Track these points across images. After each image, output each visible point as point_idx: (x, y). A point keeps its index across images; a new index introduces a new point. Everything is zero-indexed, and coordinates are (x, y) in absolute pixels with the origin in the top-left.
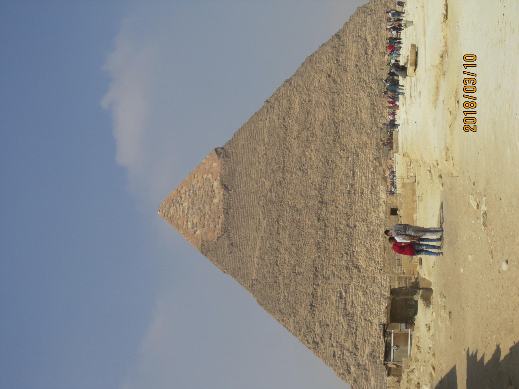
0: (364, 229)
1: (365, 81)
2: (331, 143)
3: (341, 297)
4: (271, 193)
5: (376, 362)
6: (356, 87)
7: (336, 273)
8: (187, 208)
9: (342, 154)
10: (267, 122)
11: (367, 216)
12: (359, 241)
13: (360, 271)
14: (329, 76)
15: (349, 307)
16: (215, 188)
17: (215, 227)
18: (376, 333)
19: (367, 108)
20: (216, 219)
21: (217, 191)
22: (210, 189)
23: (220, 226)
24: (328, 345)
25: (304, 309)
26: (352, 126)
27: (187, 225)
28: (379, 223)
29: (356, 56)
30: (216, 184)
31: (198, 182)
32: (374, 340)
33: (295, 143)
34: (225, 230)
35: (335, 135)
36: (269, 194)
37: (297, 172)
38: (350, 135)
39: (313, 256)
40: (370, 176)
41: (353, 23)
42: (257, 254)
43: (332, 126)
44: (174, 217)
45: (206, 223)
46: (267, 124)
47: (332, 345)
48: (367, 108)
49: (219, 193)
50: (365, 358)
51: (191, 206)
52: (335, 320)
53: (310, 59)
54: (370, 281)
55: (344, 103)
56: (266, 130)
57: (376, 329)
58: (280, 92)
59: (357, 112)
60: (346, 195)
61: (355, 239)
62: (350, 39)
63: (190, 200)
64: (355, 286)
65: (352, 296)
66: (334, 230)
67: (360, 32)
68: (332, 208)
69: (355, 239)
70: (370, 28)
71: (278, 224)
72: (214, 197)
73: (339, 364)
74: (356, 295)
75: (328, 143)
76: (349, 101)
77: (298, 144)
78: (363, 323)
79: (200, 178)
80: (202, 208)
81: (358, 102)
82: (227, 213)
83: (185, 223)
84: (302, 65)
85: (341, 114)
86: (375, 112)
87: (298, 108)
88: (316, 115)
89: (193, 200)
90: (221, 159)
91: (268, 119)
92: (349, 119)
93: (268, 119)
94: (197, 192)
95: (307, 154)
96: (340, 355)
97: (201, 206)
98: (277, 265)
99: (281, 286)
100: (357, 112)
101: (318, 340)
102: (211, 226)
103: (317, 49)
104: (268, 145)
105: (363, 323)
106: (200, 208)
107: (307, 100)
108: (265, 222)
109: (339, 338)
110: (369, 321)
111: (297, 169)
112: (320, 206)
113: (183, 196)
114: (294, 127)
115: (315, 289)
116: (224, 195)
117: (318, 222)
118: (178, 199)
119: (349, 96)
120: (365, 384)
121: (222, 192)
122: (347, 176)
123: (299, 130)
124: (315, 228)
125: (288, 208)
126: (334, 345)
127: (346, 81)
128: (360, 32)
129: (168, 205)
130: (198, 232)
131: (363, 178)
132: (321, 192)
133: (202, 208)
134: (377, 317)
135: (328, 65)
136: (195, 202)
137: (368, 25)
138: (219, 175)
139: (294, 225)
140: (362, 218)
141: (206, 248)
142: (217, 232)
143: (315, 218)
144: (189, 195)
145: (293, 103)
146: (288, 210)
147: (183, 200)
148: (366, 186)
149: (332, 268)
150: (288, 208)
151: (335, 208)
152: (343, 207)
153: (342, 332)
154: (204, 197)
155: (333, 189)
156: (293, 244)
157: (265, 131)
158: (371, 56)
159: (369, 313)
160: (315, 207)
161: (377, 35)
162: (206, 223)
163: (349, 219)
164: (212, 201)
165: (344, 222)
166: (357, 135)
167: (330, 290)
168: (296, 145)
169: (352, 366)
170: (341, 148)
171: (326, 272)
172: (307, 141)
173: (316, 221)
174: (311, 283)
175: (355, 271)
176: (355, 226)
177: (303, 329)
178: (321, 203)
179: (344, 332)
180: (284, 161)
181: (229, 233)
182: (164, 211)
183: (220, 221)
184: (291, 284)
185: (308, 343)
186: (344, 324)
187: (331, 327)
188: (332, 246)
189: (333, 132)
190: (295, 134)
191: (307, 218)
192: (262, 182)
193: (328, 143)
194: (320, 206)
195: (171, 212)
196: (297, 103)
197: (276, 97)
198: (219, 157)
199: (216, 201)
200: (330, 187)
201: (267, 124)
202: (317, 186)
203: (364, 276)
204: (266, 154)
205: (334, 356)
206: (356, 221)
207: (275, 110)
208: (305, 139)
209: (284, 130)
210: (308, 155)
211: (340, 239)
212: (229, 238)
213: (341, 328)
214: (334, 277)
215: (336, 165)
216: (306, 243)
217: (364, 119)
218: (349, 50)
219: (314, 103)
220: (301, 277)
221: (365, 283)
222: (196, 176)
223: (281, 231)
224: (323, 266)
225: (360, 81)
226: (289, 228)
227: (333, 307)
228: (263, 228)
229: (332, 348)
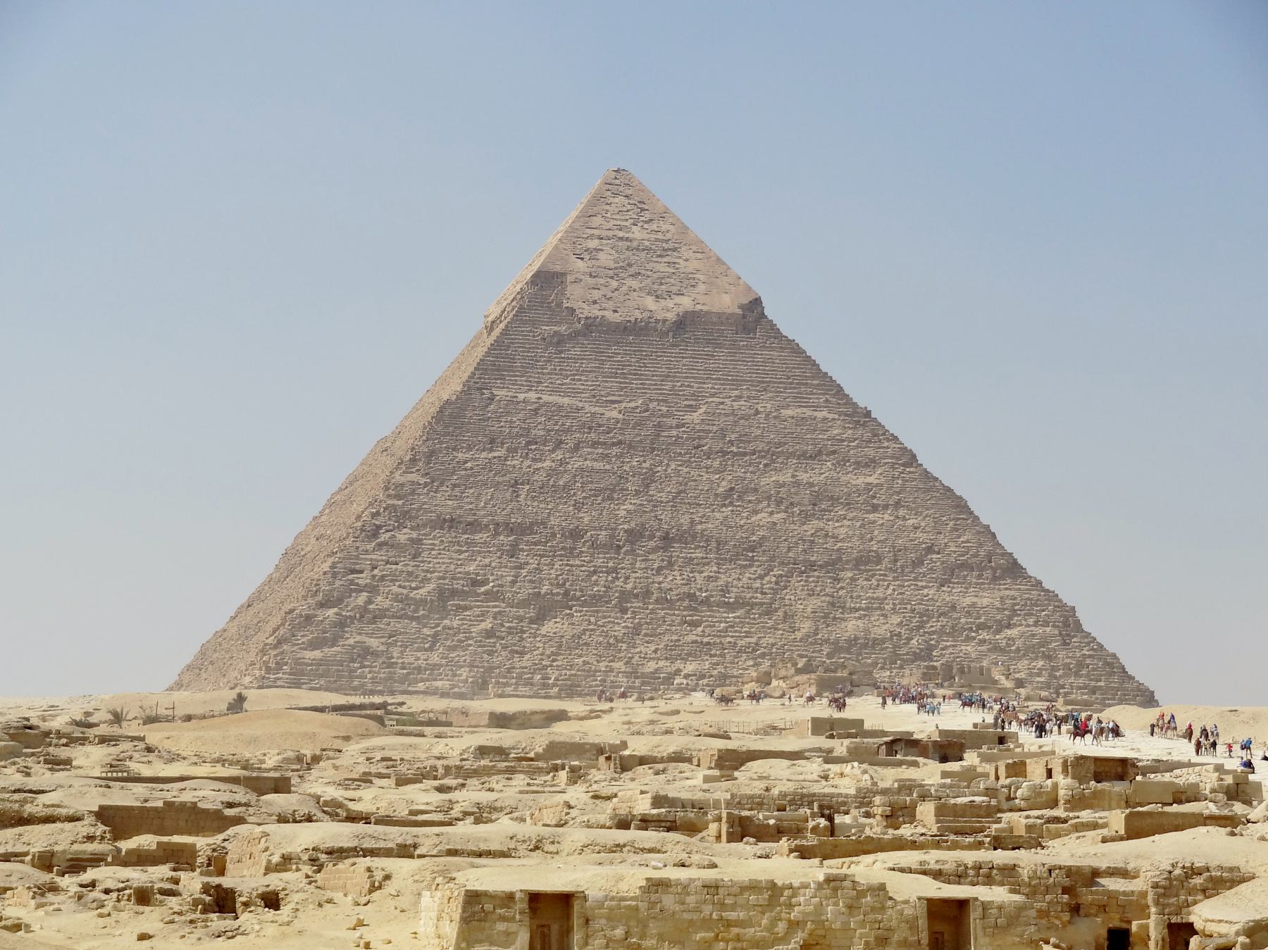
0: (619, 631)
2: (791, 554)
3: (475, 583)
4: (678, 427)
5: (353, 661)
7: (524, 572)
8: (630, 235)
9: (767, 579)
10: (824, 414)
11: (646, 635)
12: (592, 619)
13: (531, 622)
14: (930, 550)
16: (678, 299)
17: (595, 302)
18: (412, 660)
19: (867, 631)
20: (610, 305)
21: (670, 303)
22: (674, 289)
24: (374, 557)
25: (443, 503)
26: (828, 599)
27: (591, 237)
28: (634, 661)
29: (973, 605)
30: (686, 303)
31: (687, 260)
32: (395, 655)
33: (786, 477)
34: (592, 327)
36: (674, 422)
37: (724, 483)
39: (553, 521)
40: (729, 639)
41: (1042, 598)
42: (546, 398)
44: (607, 207)
45: (602, 281)
46: (820, 415)
47: (374, 568)
48: (867, 631)
49: (667, 310)
50: (358, 638)
51: (635, 244)
52: (428, 571)
53: (961, 506)
54: (515, 645)
55: (874, 582)
56: (808, 412)
57: (418, 659)
58: (888, 440)
59: (857, 610)
60: (686, 589)
61: (597, 612)
62: (1007, 592)
63: (647, 243)
64: (500, 612)
65: (478, 607)
66: (611, 564)
68: (656, 560)
69: (597, 612)
71: (614, 444)
72: (657, 297)
73: (338, 583)
74: (483, 615)
75: (789, 549)
76: (879, 593)
77: (783, 485)
78: (426, 631)
80: (632, 270)
81: (878, 612)
82: (625, 328)
83: (596, 232)
84: (949, 490)
85: (850, 574)
86: (861, 648)
87: (858, 482)
88: (846, 523)
89: (647, 249)
90: (739, 311)
91: (831, 416)
92: (841, 593)
93: (831, 416)
94: (665, 259)
95: (765, 503)
96: (357, 584)
98: (529, 443)
99: (484, 455)
101: (384, 537)
102: (596, 295)
103: (984, 520)
104: (775, 417)
105: (426, 631)
106: (630, 265)
108: (615, 414)
109: (392, 581)
110: (434, 644)
111: (730, 482)
112: (658, 534)
113: (654, 226)
114: (819, 474)
115: (487, 526)
116: (665, 321)
118: (647, 216)
119: (889, 592)
120: (305, 639)
121: (671, 316)
122: (725, 590)
123: (811, 485)
124: (613, 526)
125: (647, 465)
126: (376, 572)
129: (629, 192)
130: (580, 263)
132: (688, 537)
133: (632, 270)
134: (444, 661)
136: (643, 255)
137: (1040, 630)
138: (705, 308)
139: (613, 480)
140: (640, 624)
141: (546, 281)
142: (584, 306)
143: (633, 524)
144: (657, 240)
145: (866, 471)
146: (644, 465)
147: (646, 226)
148: (708, 631)
149: (533, 564)
150: (647, 465)
151: (656, 566)
152: (660, 583)
153: (404, 587)
154: (655, 276)
156: (575, 476)
157: (804, 410)
158: (974, 638)
159: (448, 643)
160: (655, 524)
162: (602, 281)
163: (636, 596)
164: (648, 294)
165: (629, 586)
166: (809, 610)
167: (487, 561)
168: (781, 479)
169: (336, 610)
170: (781, 576)
171: (523, 550)
172: (792, 504)
173: (626, 527)
174: (499, 519)
175: (532, 613)
176: (624, 611)
177: (400, 502)
178: (665, 538)
179: (405, 591)
180: (745, 454)
181: (585, 335)
182: (617, 182)
184: (491, 474)
185: (374, 515)
186: (421, 591)
187: (412, 563)
188: (577, 562)
190: (803, 477)
191: (631, 507)
192: (698, 407)
193: (789, 549)
194: (658, 534)
195: (616, 200)
196: (870, 480)
197: (879, 433)
198: (741, 307)
200: (699, 554)
201: (820, 415)
202: (699, 527)
203: (523, 632)
204: (757, 412)
205: (353, 571)
206: (633, 612)
207: (850, 432)
208: (796, 499)
210: (761, 506)
211: (594, 578)
212: (574, 336)
213: (413, 585)
214: (515, 568)
215: (745, 567)
216: (578, 506)
217: (844, 624)
218: (983, 590)
219: (871, 516)
220: (508, 495)
221: (509, 633)
222: (699, 256)
224: (536, 544)
225: (921, 615)
226: (608, 467)
227: (453, 567)
228: (600, 410)
229: (369, 567)
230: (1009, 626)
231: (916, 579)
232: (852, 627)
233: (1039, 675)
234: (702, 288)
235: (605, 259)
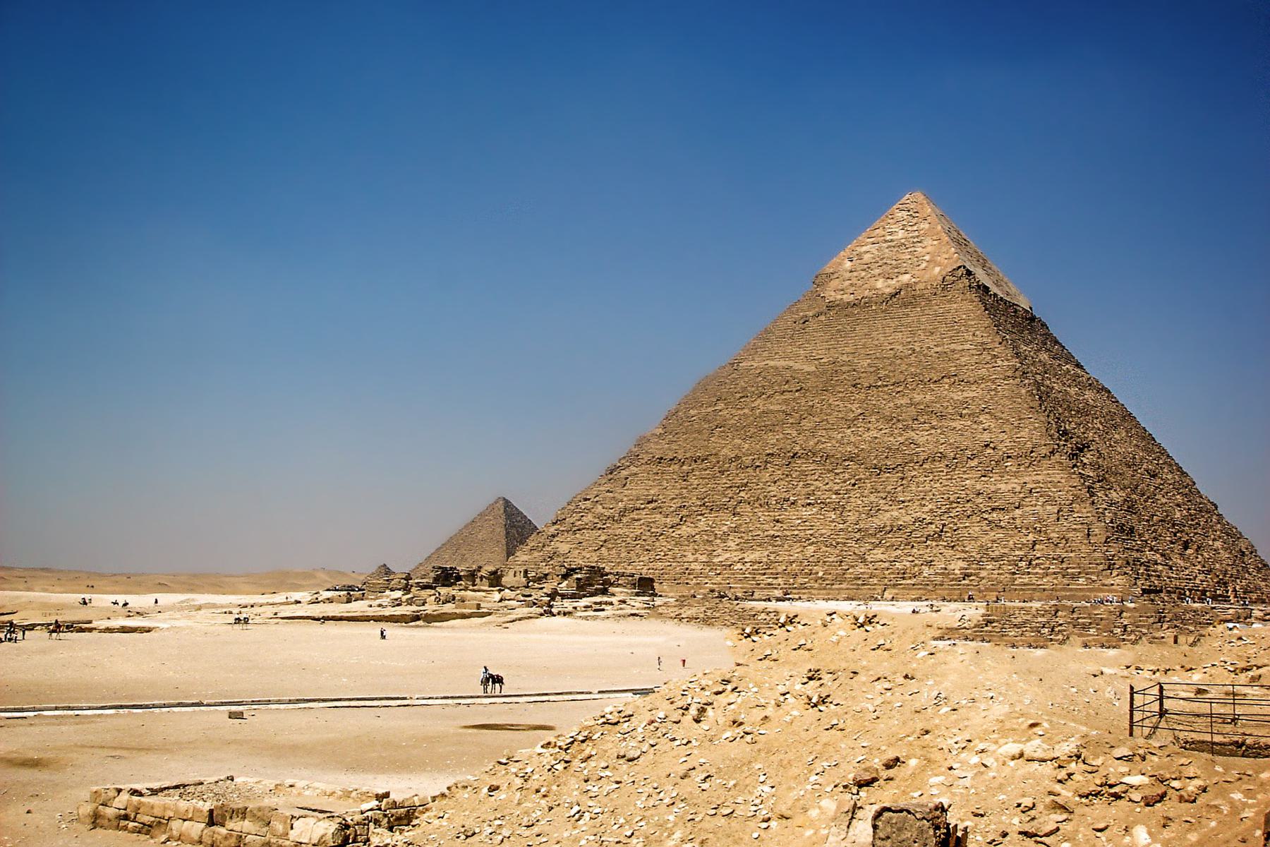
15: (634, 515)
21: (894, 282)
30: (905, 278)
43: (899, 461)
108: (813, 368)
121: (888, 290)
132: (810, 454)
190: (918, 398)
199: (880, 284)
205: (586, 500)
219: (954, 424)
223: (787, 396)
235: (867, 257)
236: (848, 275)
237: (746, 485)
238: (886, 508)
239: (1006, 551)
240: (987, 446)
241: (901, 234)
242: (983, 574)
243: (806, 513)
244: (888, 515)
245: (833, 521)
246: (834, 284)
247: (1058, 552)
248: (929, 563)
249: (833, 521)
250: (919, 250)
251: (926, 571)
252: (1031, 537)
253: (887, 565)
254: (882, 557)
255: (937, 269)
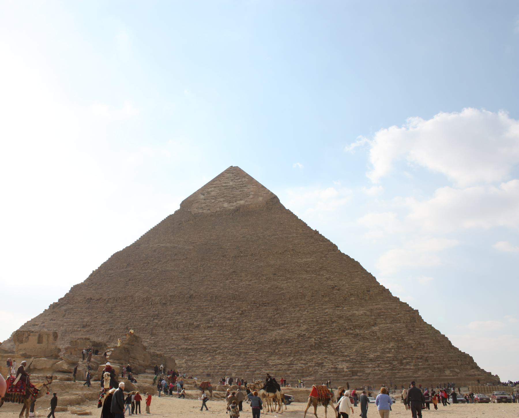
1: (320, 329)
6: (315, 320)
16: (238, 202)
21: (235, 204)
23: (201, 211)
27: (211, 188)
30: (242, 202)
35: (261, 303)
38: (257, 319)
59: (283, 324)
62: (376, 307)
67: (385, 317)
70: (388, 329)
76: (298, 315)
79: (252, 189)
97: (225, 195)
100: (283, 324)
102: (203, 205)
107: (308, 269)
113: (240, 180)
117: (171, 296)
121: (232, 208)
127: (324, 307)
128: (385, 317)
131: (204, 338)
135: (347, 285)
140: (158, 341)
152: (177, 319)
155: (202, 307)
158: (352, 334)
161: (379, 338)
183: (204, 211)
189: (264, 300)
199: (226, 205)
209: (280, 251)
225: (321, 323)
230: (375, 324)
231: (322, 304)
232: (276, 333)
233: (389, 352)
234: (251, 196)
235: (213, 193)
236: (203, 201)
237: (157, 315)
238: (271, 328)
239: (379, 354)
240: (333, 288)
241: (231, 183)
242: (368, 371)
243: (209, 333)
244: (274, 333)
245: (231, 338)
246: (195, 205)
247: (419, 354)
248: (321, 365)
249: (231, 338)
250: (246, 190)
251: (321, 371)
252: (392, 344)
253: (286, 366)
254: (280, 361)
255: (261, 199)
